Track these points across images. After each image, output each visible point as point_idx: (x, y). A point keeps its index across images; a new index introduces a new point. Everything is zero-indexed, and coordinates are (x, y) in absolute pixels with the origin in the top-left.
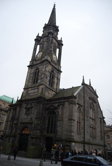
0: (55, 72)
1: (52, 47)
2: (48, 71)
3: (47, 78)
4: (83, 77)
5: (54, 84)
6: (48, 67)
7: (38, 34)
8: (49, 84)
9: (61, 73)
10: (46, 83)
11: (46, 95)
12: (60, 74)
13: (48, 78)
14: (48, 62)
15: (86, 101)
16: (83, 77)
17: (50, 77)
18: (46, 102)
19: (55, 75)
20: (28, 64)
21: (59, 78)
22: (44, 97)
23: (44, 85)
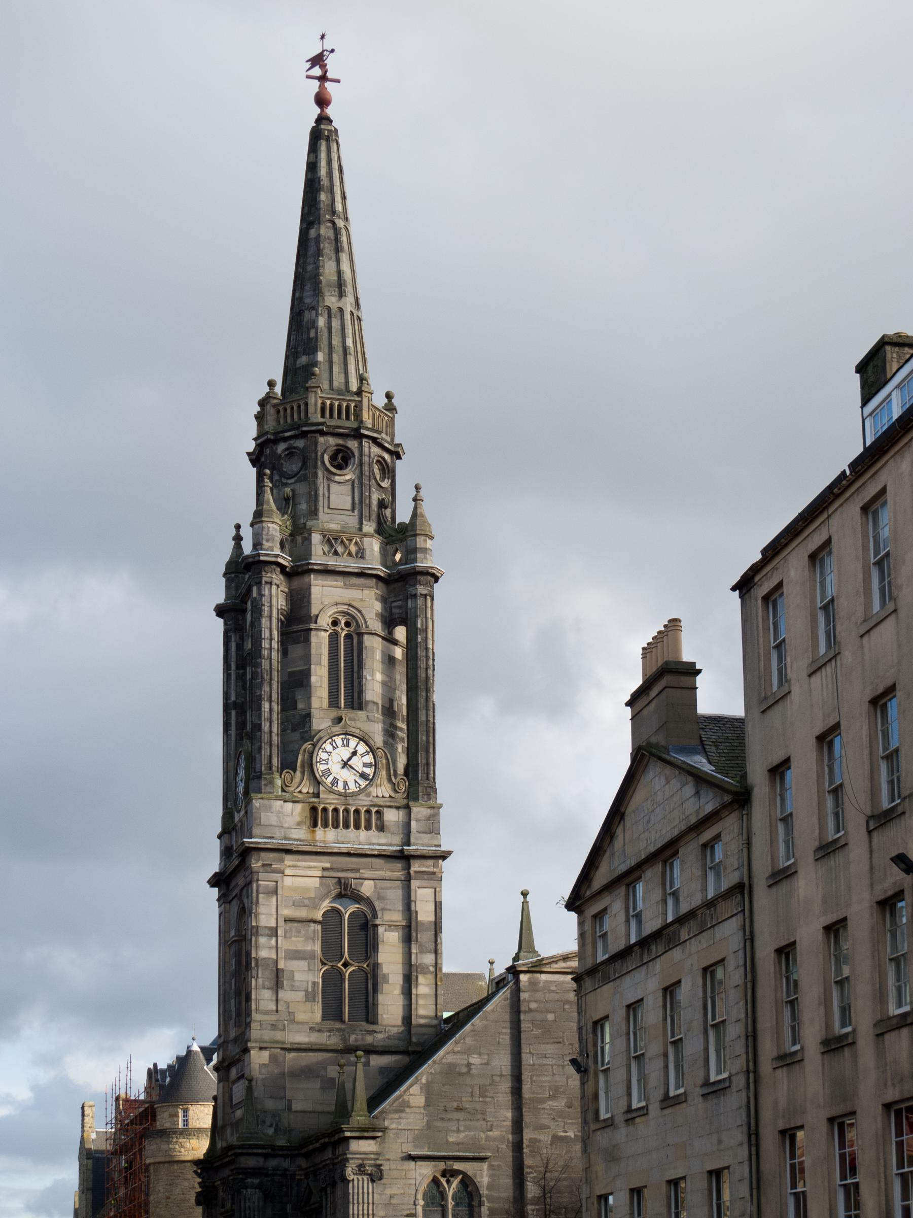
0: (367, 889)
1: (307, 674)
2: (286, 921)
3: (278, 980)
4: (525, 904)
5: (375, 989)
6: (275, 892)
7: (238, 539)
8: (332, 1010)
9: (444, 864)
10: (274, 1027)
11: (296, 1106)
12: (434, 878)
13: (306, 975)
14: (272, 855)
15: (552, 1097)
16: (525, 904)
17: (331, 949)
18: (303, 1163)
19: (375, 915)
20: (213, 865)
21: (425, 913)
22: (271, 1131)
23: (261, 1049)
